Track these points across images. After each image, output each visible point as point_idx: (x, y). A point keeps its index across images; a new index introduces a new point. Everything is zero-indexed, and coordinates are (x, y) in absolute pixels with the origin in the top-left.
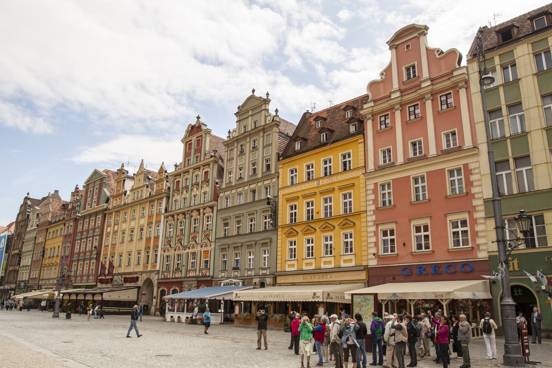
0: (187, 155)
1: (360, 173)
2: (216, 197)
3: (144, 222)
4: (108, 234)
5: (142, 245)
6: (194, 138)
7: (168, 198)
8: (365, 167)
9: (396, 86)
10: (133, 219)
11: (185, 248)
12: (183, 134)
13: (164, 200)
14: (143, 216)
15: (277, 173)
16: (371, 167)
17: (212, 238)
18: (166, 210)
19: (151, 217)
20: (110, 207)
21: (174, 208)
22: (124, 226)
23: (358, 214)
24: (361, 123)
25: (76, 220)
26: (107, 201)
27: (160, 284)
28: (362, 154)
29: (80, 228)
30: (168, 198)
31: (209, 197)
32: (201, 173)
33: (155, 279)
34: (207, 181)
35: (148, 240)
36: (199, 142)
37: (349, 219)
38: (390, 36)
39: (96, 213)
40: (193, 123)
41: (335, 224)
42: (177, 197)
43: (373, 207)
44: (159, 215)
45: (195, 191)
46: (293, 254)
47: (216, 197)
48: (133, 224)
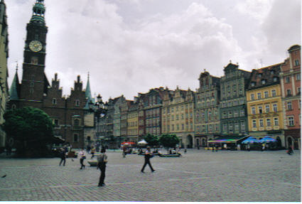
0: (202, 85)
1: (279, 98)
2: (218, 103)
3: (183, 112)
4: (164, 117)
5: (184, 121)
6: (204, 79)
7: (195, 102)
8: (281, 95)
9: (291, 67)
10: (177, 111)
11: (206, 122)
12: (199, 77)
13: (193, 104)
14: (182, 109)
15: (245, 95)
16: (284, 95)
17: (219, 118)
18: (195, 108)
19: (187, 110)
20: (163, 105)
21: (198, 107)
22: (172, 114)
23: (280, 111)
24: (279, 79)
25: (144, 111)
26: (161, 103)
27: (195, 137)
28: (279, 91)
29: (147, 114)
30: (195, 102)
31: (215, 104)
32: (210, 93)
33: (193, 135)
34: (213, 96)
35: (187, 119)
36: (207, 80)
37: (276, 114)
38: (288, 48)
39: (156, 108)
40: (203, 72)
41: (271, 114)
42: (199, 102)
43: (285, 110)
44: (191, 109)
45: (208, 100)
46: (255, 125)
47: (218, 103)
48: (177, 113)
